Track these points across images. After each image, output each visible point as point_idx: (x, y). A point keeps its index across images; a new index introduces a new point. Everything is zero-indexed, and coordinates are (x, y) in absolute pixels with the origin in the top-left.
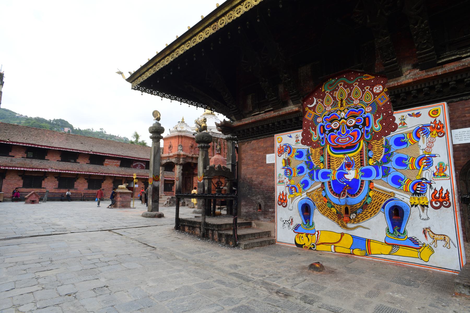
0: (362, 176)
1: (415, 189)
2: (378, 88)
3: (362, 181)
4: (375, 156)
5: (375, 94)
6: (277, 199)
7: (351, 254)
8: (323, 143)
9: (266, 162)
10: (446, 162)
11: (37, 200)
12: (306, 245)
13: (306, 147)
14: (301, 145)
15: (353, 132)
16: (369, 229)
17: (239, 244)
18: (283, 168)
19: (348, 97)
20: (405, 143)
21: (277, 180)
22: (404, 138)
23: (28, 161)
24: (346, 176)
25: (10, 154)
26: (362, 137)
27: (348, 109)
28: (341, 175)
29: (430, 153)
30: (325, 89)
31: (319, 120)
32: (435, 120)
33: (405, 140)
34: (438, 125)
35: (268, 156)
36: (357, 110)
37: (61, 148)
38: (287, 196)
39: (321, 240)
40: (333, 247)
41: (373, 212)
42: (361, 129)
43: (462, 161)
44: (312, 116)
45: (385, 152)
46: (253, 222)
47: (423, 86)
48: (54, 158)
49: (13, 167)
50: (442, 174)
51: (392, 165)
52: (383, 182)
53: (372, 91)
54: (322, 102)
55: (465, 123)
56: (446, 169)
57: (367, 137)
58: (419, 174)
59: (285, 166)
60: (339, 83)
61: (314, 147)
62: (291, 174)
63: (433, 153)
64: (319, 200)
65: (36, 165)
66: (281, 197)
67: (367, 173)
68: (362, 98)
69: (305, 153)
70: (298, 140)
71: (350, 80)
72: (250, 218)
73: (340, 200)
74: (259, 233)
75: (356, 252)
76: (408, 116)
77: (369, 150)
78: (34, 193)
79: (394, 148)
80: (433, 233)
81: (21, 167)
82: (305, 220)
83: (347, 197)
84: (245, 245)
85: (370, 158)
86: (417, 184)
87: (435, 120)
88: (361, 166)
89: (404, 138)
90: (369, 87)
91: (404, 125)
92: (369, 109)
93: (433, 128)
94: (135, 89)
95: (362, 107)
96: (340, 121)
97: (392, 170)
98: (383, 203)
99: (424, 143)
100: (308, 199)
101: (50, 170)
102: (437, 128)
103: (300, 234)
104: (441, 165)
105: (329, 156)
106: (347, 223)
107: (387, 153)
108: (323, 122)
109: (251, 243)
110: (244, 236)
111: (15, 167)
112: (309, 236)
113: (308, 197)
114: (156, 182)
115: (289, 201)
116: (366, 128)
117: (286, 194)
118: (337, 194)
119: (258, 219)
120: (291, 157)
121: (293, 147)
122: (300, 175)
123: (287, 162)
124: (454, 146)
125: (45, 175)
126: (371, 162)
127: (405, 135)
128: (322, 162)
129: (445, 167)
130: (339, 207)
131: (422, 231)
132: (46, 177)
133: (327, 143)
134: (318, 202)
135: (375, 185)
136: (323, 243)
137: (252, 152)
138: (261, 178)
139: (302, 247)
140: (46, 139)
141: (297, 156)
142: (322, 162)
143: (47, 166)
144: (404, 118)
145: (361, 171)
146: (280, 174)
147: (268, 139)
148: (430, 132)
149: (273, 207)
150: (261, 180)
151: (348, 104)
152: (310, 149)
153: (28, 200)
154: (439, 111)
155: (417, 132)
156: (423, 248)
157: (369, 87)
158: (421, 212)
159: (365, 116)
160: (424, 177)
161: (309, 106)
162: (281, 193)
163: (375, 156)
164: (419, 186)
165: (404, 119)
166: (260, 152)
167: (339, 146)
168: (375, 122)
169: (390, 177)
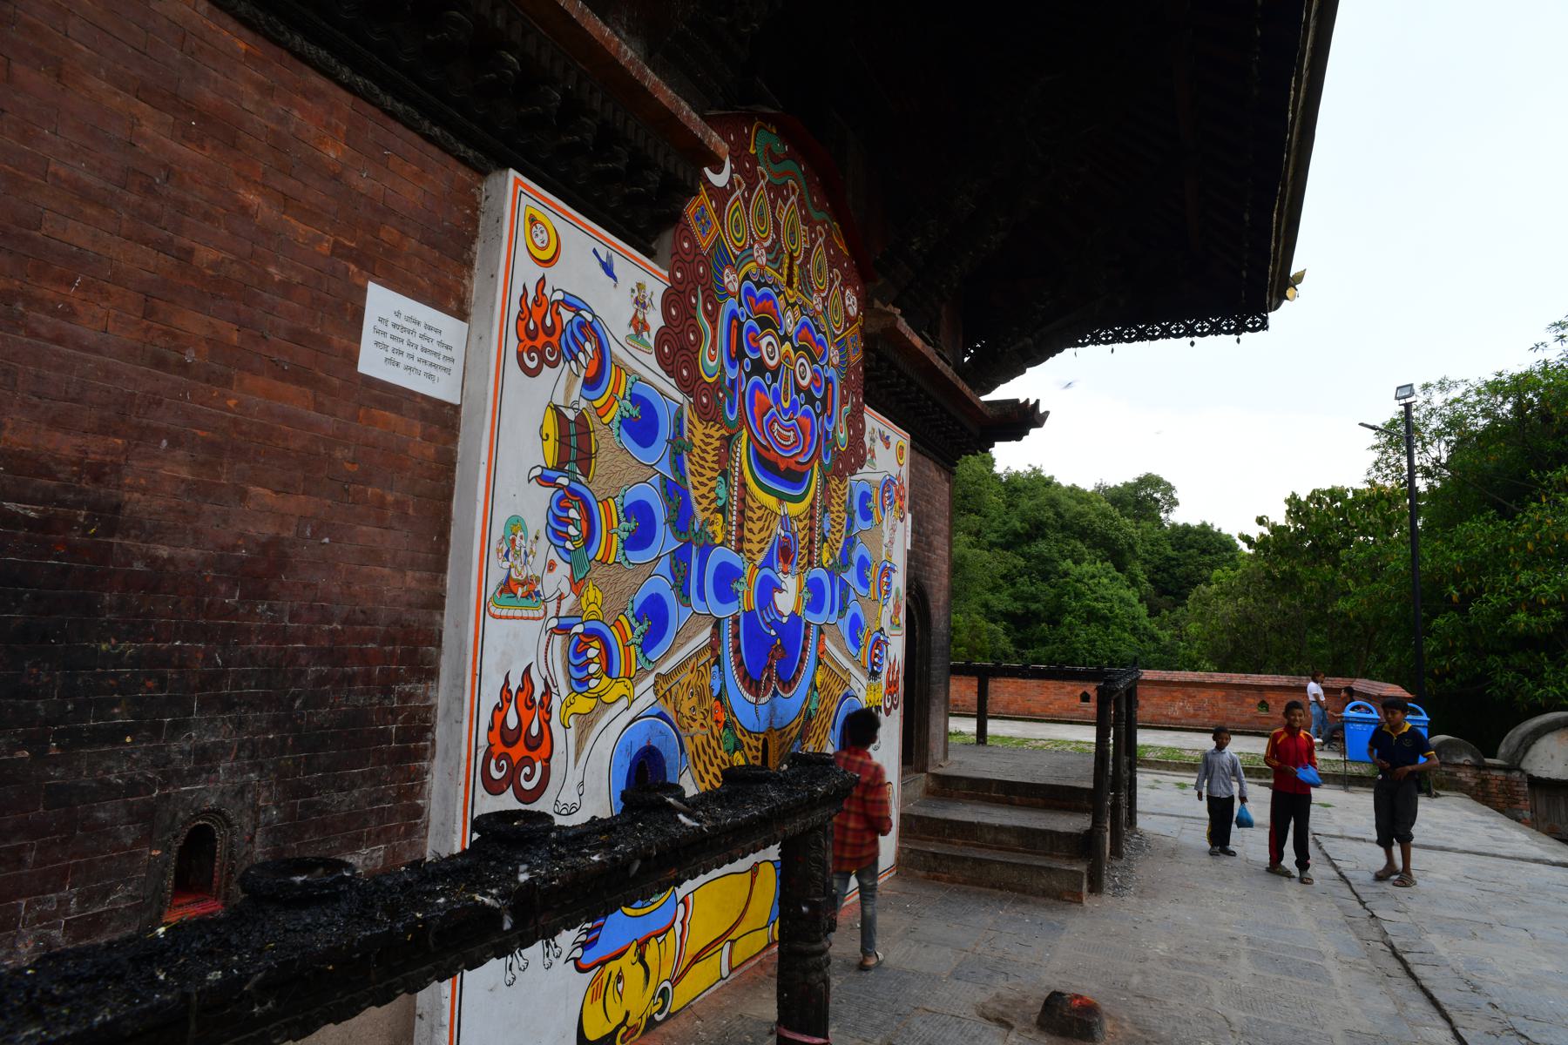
0: (808, 607)
3: (808, 625)
8: (732, 412)
9: (352, 357)
12: (630, 1023)
13: (669, 387)
14: (652, 360)
18: (544, 480)
21: (474, 568)
24: (777, 595)
28: (768, 589)
38: (555, 702)
42: (818, 416)
54: (747, 202)
59: (559, 468)
62: (589, 540)
64: (699, 717)
66: (512, 722)
67: (815, 596)
69: (665, 430)
70: (646, 327)
83: (775, 694)
88: (810, 563)
97: (852, 596)
98: (835, 706)
100: (662, 716)
105: (743, 485)
108: (740, 305)
113: (661, 706)
115: (563, 739)
117: (547, 693)
118: (753, 683)
120: (600, 413)
122: (636, 557)
123: (573, 442)
128: (721, 510)
130: (753, 743)
133: (742, 420)
134: (696, 726)
135: (827, 642)
136: (696, 959)
138: (262, 513)
141: (627, 423)
146: (516, 524)
147: (402, 139)
150: (267, 529)
152: (687, 411)
162: (514, 686)
167: (770, 456)
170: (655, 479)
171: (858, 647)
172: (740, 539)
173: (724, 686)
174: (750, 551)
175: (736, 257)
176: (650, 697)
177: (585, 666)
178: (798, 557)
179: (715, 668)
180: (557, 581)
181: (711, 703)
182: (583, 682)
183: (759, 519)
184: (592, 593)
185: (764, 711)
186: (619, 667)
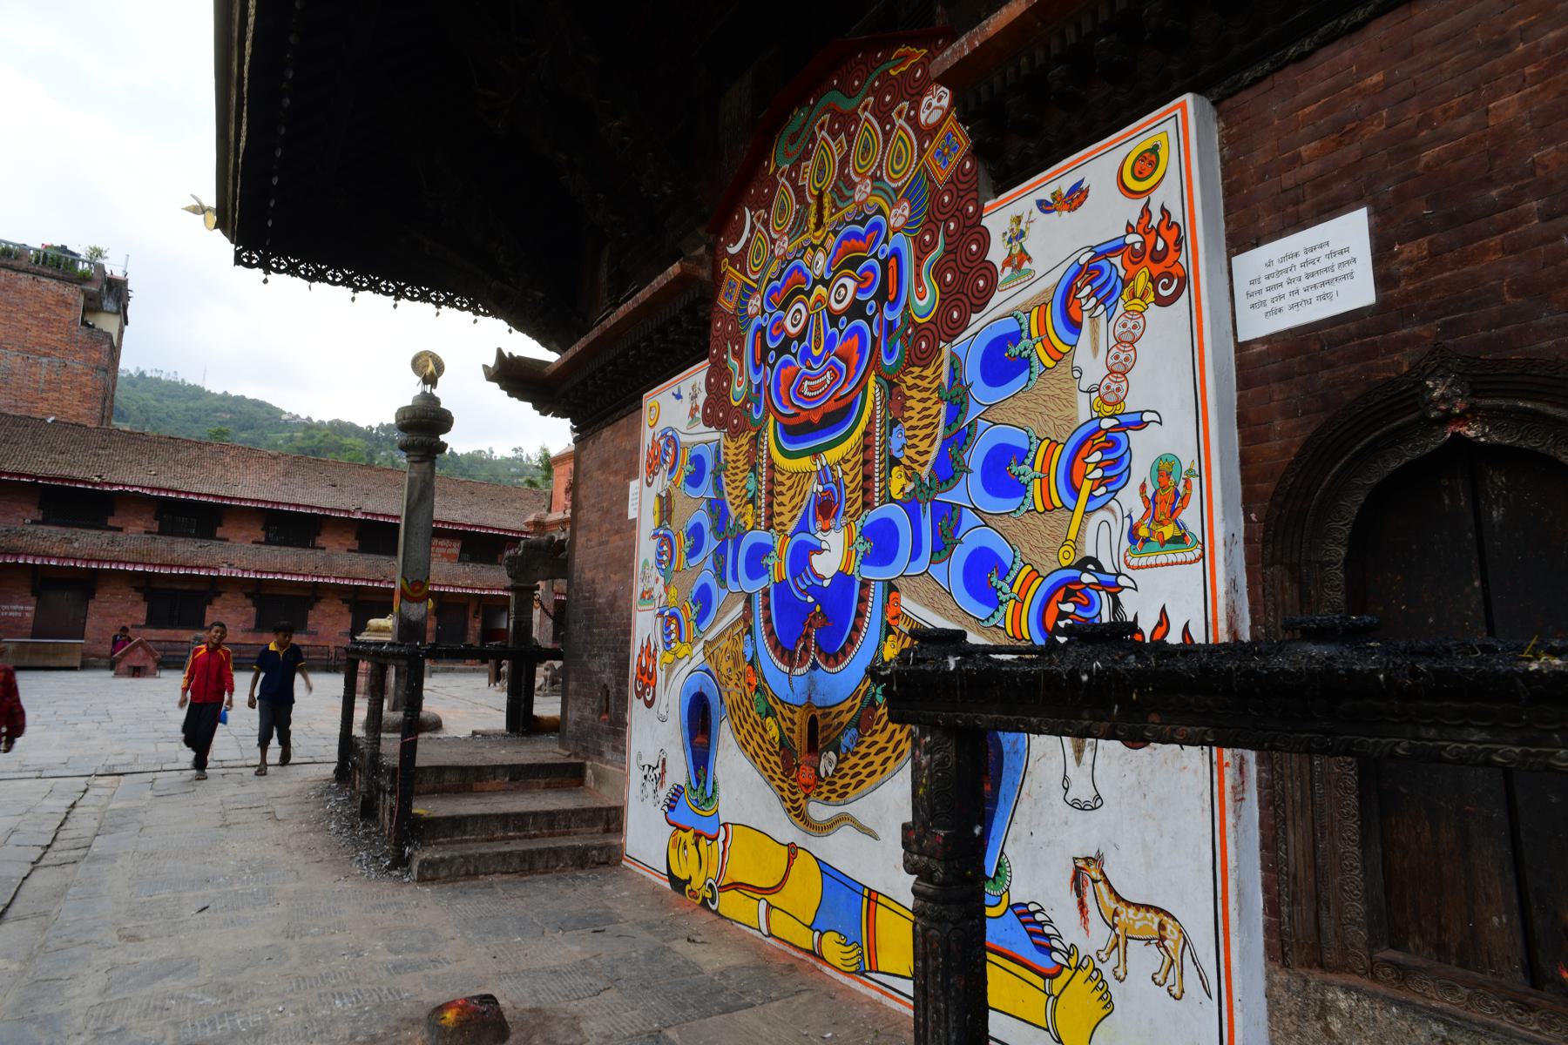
0: (867, 560)
1: (1050, 626)
2: (935, 103)
3: (865, 584)
4: (911, 453)
5: (925, 133)
6: (633, 669)
7: (811, 953)
10: (1188, 459)
11: (151, 664)
13: (714, 435)
14: (701, 427)
15: (845, 339)
16: (876, 838)
17: (411, 855)
18: (655, 536)
19: (839, 178)
20: (1023, 363)
22: (1015, 338)
23: (162, 543)
24: (816, 560)
25: (111, 522)
26: (874, 363)
27: (835, 233)
28: (802, 555)
29: (1119, 409)
30: (779, 164)
31: (754, 305)
32: (1146, 211)
33: (1021, 346)
34: (1158, 234)
35: (634, 485)
36: (862, 230)
37: (258, 501)
39: (736, 873)
40: (763, 904)
41: (891, 746)
42: (869, 320)
43: (1276, 443)
44: (736, 293)
45: (948, 426)
46: (589, 763)
47: (1087, 27)
48: (245, 533)
49: (111, 562)
50: (1169, 531)
51: (968, 491)
52: (932, 586)
53: (914, 122)
54: (766, 223)
55: (1296, 202)
56: (1185, 499)
57: (889, 356)
58: (1072, 536)
60: (814, 123)
61: (734, 434)
62: (671, 561)
63: (1132, 404)
64: (734, 677)
65: (189, 556)
67: (881, 542)
68: (880, 166)
69: (709, 466)
70: (697, 408)
71: (850, 93)
72: (585, 749)
73: (794, 679)
74: (549, 814)
75: (832, 947)
76: (1037, 212)
77: (894, 423)
78: (140, 643)
79: (981, 394)
80: (1112, 890)
81: (135, 563)
82: (696, 770)
83: (815, 666)
84: (427, 865)
85: (895, 462)
86: (1062, 592)
87: (1146, 211)
88: (867, 505)
89: (1015, 338)
90: (906, 104)
91: (1018, 268)
92: (899, 215)
93: (1135, 257)
94: (249, 265)
95: (880, 211)
96: (809, 294)
97: (969, 519)
99: (1095, 350)
100: (708, 671)
101: (223, 573)
102: (1157, 257)
103: (681, 833)
104: (1164, 469)
105: (772, 466)
106: (807, 796)
107: (955, 427)
109: (466, 858)
110: (457, 824)
111: (119, 562)
112: (703, 842)
113: (708, 665)
114: (415, 606)
115: (661, 676)
116: (889, 315)
118: (786, 652)
119: (601, 754)
121: (683, 438)
122: (694, 561)
123: (666, 507)
124: (1241, 347)
125: (216, 587)
126: (898, 483)
127: (1024, 319)
128: (752, 501)
129: (1181, 489)
130: (787, 714)
131: (1070, 874)
132: (218, 594)
134: (731, 685)
135: (905, 602)
136: (736, 886)
137: (598, 475)
139: (683, 893)
140: (219, 471)
142: (752, 501)
143: (219, 559)
144: (1023, 226)
145: (867, 532)
146: (646, 562)
148: (1125, 283)
149: (623, 701)
150: (613, 589)
151: (839, 210)
153: (122, 665)
154: (1162, 153)
155: (1070, 291)
156: (1067, 974)
157: (906, 104)
158: (1071, 760)
159: (888, 251)
160: (1090, 552)
161: (733, 250)
163: (911, 453)
164: (1069, 608)
165: (1022, 234)
166: (617, 473)
168: (918, 275)
169: (960, 555)
170: (704, 505)
171: (997, 604)
172: (770, 518)
173: (755, 654)
174: (782, 524)
175: (756, 281)
176: (701, 657)
177: (668, 636)
178: (844, 506)
179: (748, 637)
180: (658, 589)
181: (744, 667)
182: (669, 644)
183: (790, 488)
184: (673, 591)
185: (800, 684)
186: (685, 637)
